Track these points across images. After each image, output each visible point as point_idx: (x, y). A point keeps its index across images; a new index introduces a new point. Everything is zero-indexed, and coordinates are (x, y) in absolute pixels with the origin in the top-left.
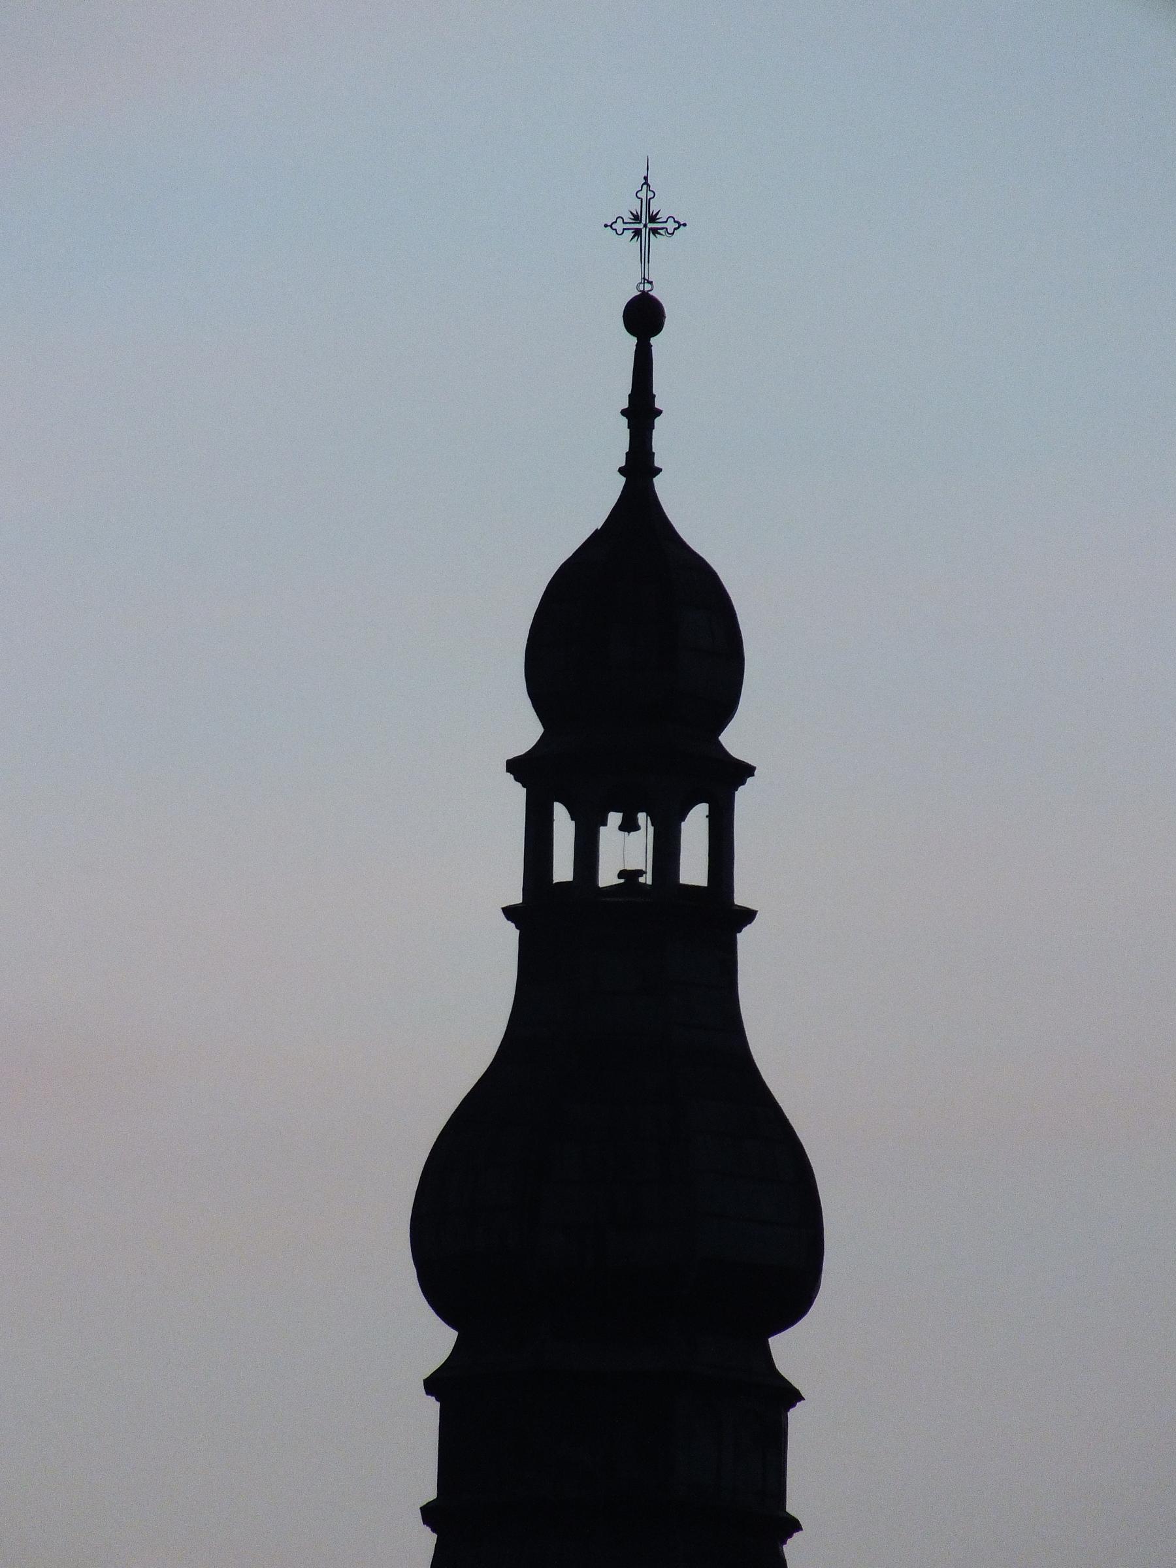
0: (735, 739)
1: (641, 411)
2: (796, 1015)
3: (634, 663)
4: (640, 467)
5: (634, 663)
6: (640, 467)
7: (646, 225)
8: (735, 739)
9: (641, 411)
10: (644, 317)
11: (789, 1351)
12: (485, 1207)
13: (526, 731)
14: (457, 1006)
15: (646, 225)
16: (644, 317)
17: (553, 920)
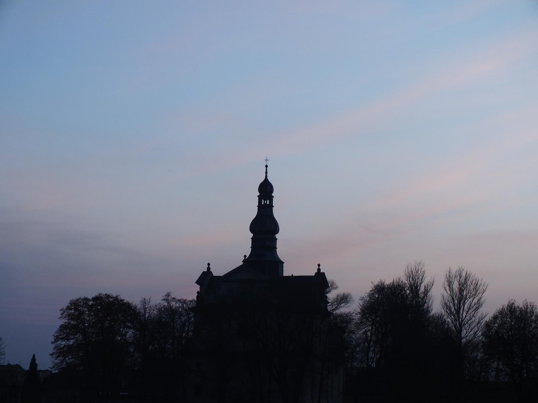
0: (273, 195)
1: (266, 173)
2: (278, 213)
3: (266, 190)
4: (266, 176)
5: (266, 190)
6: (266, 176)
7: (267, 160)
8: (273, 195)
9: (266, 173)
10: (267, 166)
11: (277, 236)
12: (254, 227)
13: (258, 194)
14: (253, 212)
15: (267, 160)
16: (267, 166)
17: (260, 206)
